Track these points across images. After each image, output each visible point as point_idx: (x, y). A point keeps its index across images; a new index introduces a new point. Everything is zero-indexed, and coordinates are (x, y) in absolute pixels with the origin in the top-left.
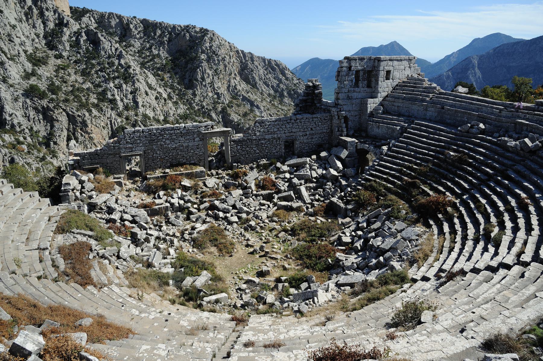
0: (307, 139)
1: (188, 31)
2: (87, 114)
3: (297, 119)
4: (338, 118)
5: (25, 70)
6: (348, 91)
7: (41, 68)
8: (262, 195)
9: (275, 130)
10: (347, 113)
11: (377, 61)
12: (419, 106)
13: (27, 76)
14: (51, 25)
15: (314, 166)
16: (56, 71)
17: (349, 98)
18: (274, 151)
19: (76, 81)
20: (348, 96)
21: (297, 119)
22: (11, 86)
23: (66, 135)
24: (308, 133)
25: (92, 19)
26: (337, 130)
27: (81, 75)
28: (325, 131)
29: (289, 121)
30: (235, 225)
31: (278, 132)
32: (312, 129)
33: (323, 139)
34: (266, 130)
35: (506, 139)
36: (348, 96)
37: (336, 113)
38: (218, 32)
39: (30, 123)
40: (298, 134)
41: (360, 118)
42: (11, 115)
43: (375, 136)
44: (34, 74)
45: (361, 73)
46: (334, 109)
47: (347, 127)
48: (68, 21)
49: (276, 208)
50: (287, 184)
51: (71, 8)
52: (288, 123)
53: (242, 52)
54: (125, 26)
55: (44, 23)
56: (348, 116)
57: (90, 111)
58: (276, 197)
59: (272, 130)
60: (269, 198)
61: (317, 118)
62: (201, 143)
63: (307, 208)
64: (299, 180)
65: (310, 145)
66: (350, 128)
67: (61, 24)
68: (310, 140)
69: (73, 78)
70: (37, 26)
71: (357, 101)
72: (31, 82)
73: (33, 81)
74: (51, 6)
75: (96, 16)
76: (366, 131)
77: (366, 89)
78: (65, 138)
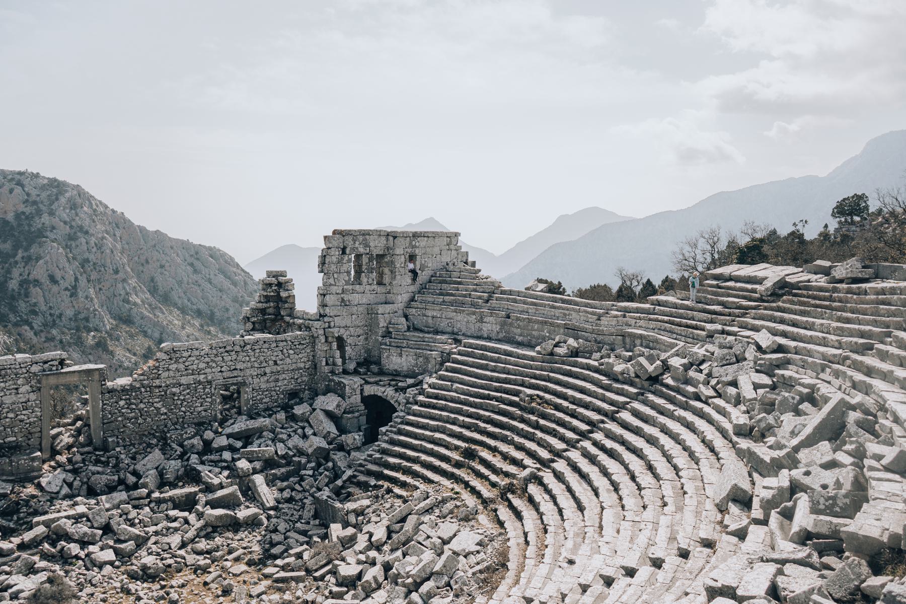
0: (268, 381)
1: (19, 183)
3: (246, 344)
4: (326, 341)
6: (343, 292)
8: (171, 499)
9: (202, 365)
10: (342, 331)
11: (391, 239)
12: (468, 314)
15: (282, 433)
18: (200, 409)
21: (246, 344)
24: (268, 370)
26: (324, 363)
28: (302, 365)
29: (228, 348)
30: (108, 569)
31: (208, 370)
32: (276, 363)
33: (299, 380)
34: (182, 367)
35: (611, 360)
37: (321, 332)
38: (89, 188)
40: (248, 372)
41: (366, 339)
43: (396, 370)
45: (365, 260)
46: (317, 324)
47: (343, 357)
49: (202, 523)
50: (226, 473)
52: (227, 352)
53: (142, 229)
56: (345, 337)
58: (202, 498)
59: (195, 367)
60: (188, 504)
61: (286, 341)
62: (33, 396)
63: (269, 518)
64: (250, 462)
65: (273, 393)
66: (350, 358)
68: (272, 384)
71: (361, 309)
76: (378, 363)
77: (375, 287)
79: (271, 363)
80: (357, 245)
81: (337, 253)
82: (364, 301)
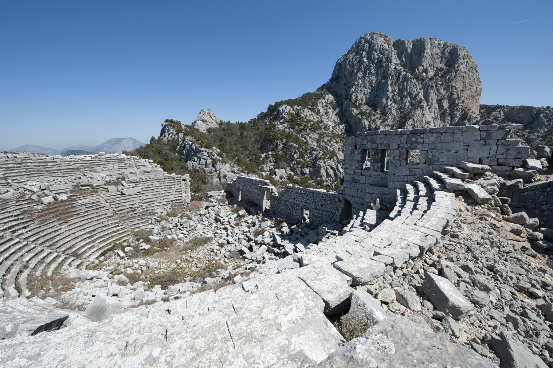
6: (354, 173)
9: (296, 197)
14: (457, 119)
17: (354, 181)
20: (354, 179)
24: (318, 208)
25: (502, 112)
36: (354, 179)
51: (482, 107)
54: (534, 115)
55: (452, 119)
62: (260, 192)
68: (320, 215)
70: (446, 120)
74: (461, 108)
75: (506, 110)
79: (320, 204)
80: (365, 143)
81: (351, 148)
82: (369, 182)
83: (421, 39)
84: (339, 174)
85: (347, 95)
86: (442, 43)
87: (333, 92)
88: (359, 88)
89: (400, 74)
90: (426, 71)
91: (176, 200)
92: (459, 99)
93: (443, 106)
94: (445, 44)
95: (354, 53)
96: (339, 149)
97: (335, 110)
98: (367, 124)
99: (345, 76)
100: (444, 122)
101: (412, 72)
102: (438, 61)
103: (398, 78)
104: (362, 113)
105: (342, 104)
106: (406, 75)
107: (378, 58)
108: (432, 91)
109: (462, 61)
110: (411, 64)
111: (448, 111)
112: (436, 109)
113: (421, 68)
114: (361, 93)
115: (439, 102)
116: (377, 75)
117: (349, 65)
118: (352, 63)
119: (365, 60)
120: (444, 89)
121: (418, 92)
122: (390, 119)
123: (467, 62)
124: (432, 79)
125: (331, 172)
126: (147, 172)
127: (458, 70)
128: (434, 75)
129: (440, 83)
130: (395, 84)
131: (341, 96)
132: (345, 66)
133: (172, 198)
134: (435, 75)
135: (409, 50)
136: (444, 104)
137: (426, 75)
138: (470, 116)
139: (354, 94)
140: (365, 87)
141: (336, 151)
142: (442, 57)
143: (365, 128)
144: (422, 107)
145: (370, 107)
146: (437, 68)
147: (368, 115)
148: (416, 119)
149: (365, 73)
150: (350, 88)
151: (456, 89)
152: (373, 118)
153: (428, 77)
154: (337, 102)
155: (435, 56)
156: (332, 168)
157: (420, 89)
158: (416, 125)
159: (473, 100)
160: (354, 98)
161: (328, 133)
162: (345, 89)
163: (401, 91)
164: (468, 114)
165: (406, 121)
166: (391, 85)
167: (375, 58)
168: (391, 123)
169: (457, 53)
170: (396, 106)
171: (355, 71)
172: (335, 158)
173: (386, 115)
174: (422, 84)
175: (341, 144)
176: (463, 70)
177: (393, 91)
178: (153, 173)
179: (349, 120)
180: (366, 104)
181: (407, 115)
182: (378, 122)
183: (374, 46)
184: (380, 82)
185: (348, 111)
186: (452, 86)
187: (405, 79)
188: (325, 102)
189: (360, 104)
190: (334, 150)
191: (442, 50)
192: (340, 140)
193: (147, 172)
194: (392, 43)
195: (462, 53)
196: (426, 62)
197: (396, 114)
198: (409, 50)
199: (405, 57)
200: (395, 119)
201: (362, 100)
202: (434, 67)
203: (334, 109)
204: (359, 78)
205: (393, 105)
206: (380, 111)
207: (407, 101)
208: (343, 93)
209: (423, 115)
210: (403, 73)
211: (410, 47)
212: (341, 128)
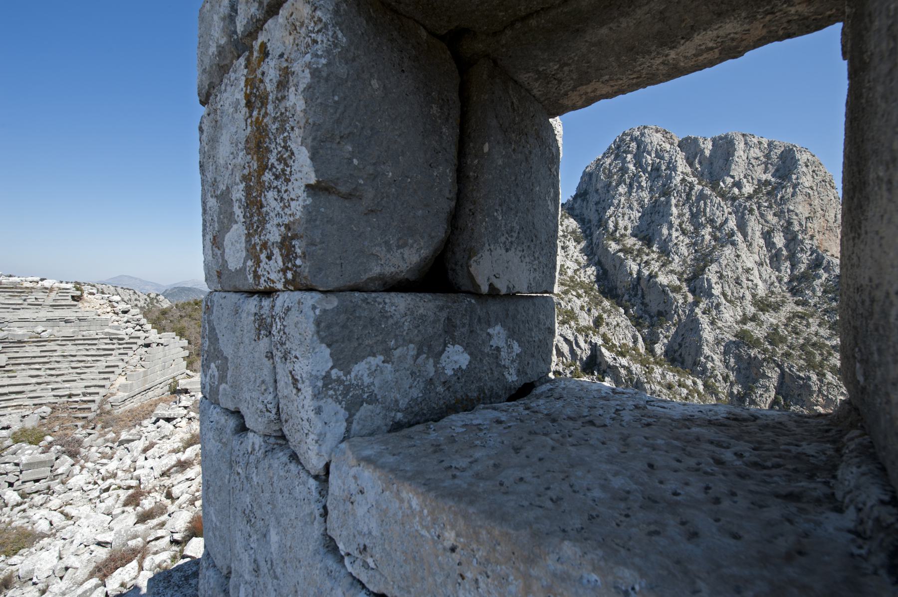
2: (814, 377)
5: (744, 314)
7: (767, 314)
13: (744, 320)
14: (803, 267)
16: (789, 319)
19: (816, 334)
22: (719, 328)
23: (773, 397)
27: (830, 328)
39: (726, 371)
42: (707, 358)
44: (754, 318)
48: (829, 262)
55: (793, 266)
57: (821, 375)
67: (817, 263)
69: (813, 329)
70: (783, 268)
72: (745, 327)
73: (749, 326)
74: (808, 247)
78: (769, 401)
83: (726, 137)
84: (579, 352)
85: (600, 220)
86: (765, 141)
87: (577, 216)
88: (620, 210)
89: (691, 189)
90: (738, 185)
91: (84, 395)
92: (805, 231)
93: (774, 243)
94: (770, 144)
95: (613, 157)
96: (582, 308)
97: (579, 243)
98: (635, 268)
99: (597, 191)
100: (779, 270)
101: (713, 189)
102: (760, 169)
103: (689, 195)
104: (626, 250)
105: (591, 234)
106: (702, 190)
107: (653, 164)
108: (753, 218)
109: (804, 169)
110: (710, 173)
111: (785, 253)
112: (762, 248)
113: (729, 180)
114: (624, 218)
115: (767, 236)
116: (651, 190)
117: (605, 174)
118: (610, 171)
119: (631, 167)
120: (775, 215)
121: (727, 219)
122: (677, 261)
123: (814, 171)
124: (750, 197)
125: (565, 349)
126: (67, 321)
127: (799, 184)
128: (754, 191)
129: (766, 204)
130: (683, 205)
131: (590, 221)
132: (598, 176)
133: (77, 388)
134: (756, 191)
135: (707, 153)
136: (775, 240)
137: (740, 191)
138: (829, 262)
139: (612, 219)
140: (631, 208)
141: (577, 310)
142: (766, 164)
143: (631, 274)
144: (734, 244)
145: (640, 239)
146: (759, 181)
147: (635, 253)
148: (724, 263)
149: (631, 186)
150: (605, 210)
151: (797, 215)
152: (645, 258)
153: (742, 195)
154: (584, 232)
155: (753, 161)
156: (566, 340)
157: (730, 213)
158: (725, 273)
159: (831, 234)
160: (611, 225)
161: (564, 280)
162: (597, 211)
163: (694, 216)
164: (823, 258)
165: (705, 266)
166: (676, 206)
167: (648, 164)
168: (679, 269)
169: (794, 157)
170: (687, 241)
171: (614, 184)
172: (572, 323)
173: (668, 255)
174: (732, 205)
175: (587, 299)
176: (807, 184)
177: (680, 215)
178: (83, 323)
179: (603, 260)
180: (634, 235)
181: (707, 255)
182: (655, 266)
183: (645, 147)
184: (656, 201)
185: (600, 246)
186: (789, 211)
187: (702, 196)
188: (563, 231)
189: (623, 236)
190: (572, 309)
191: (766, 152)
192: (585, 292)
193: (67, 321)
194: (676, 142)
195: (802, 157)
196: (738, 171)
197: (686, 254)
198: (707, 153)
199: (700, 163)
200: (684, 261)
201: (626, 229)
202: (752, 179)
203: (578, 241)
204: (620, 195)
205: (681, 238)
206: (658, 248)
207: (706, 232)
208: (594, 217)
209: (738, 256)
210: (698, 188)
211: (707, 148)
212: (588, 273)
